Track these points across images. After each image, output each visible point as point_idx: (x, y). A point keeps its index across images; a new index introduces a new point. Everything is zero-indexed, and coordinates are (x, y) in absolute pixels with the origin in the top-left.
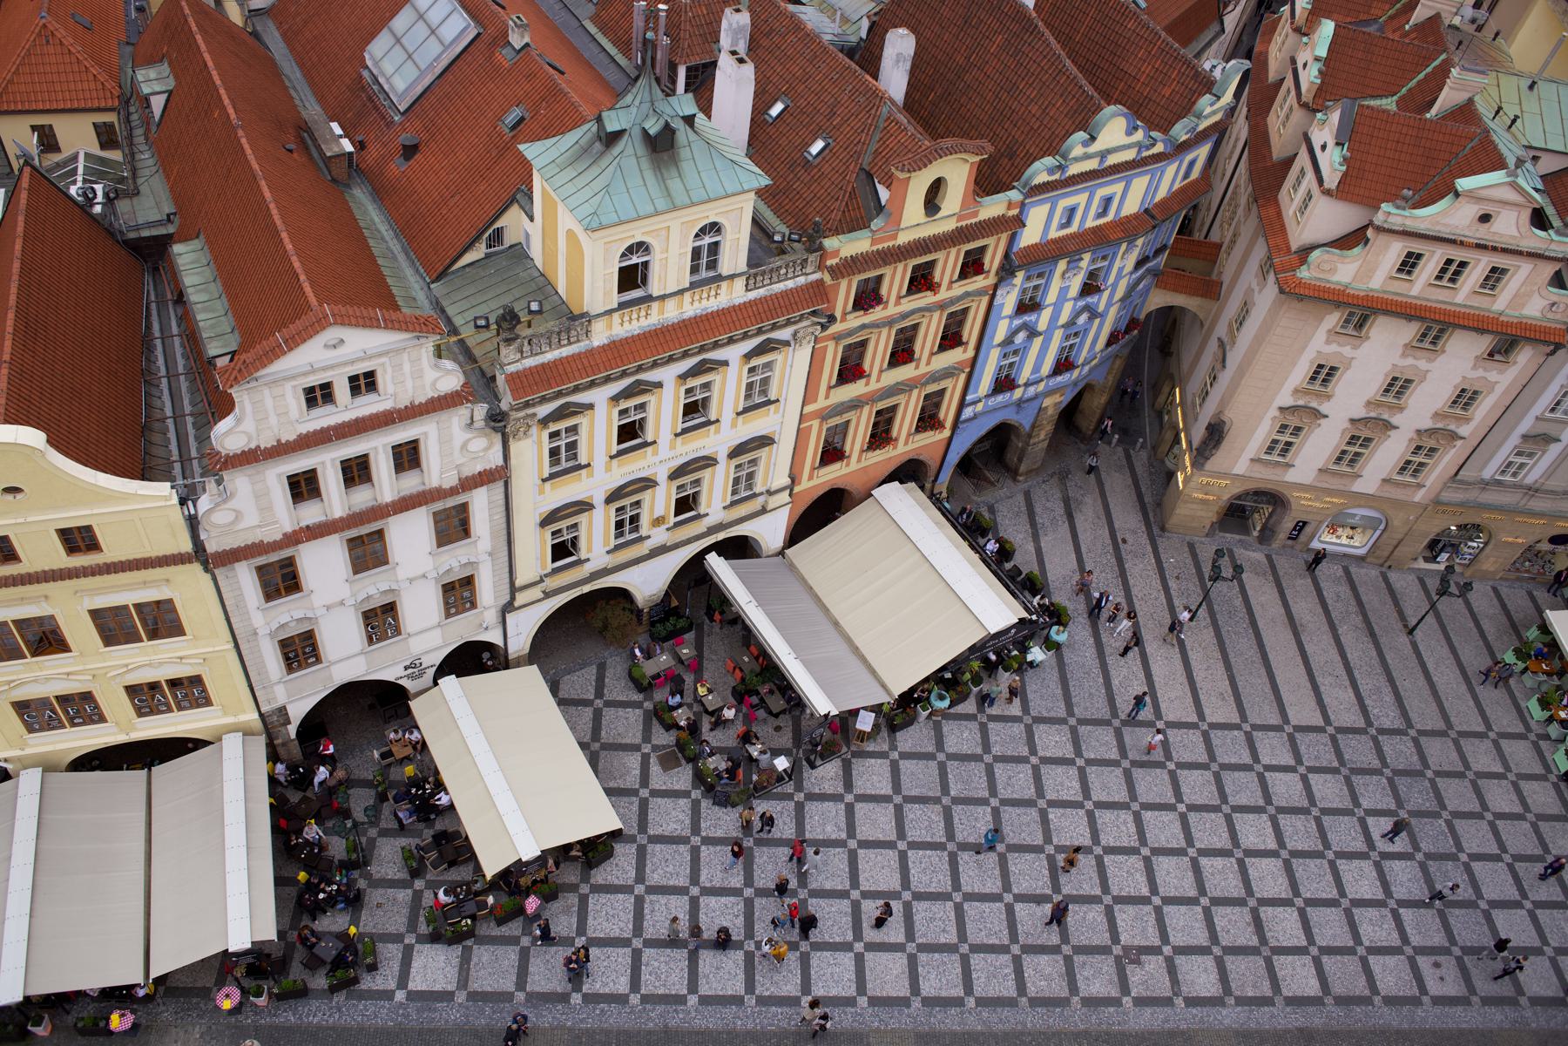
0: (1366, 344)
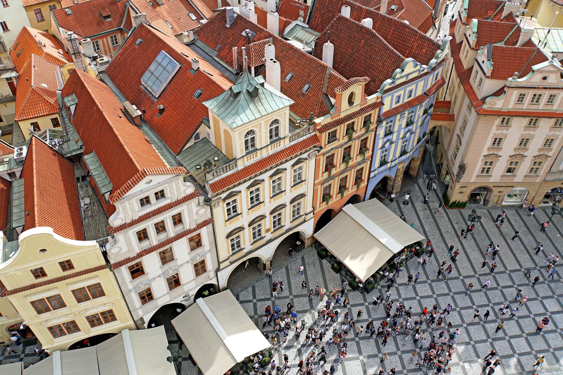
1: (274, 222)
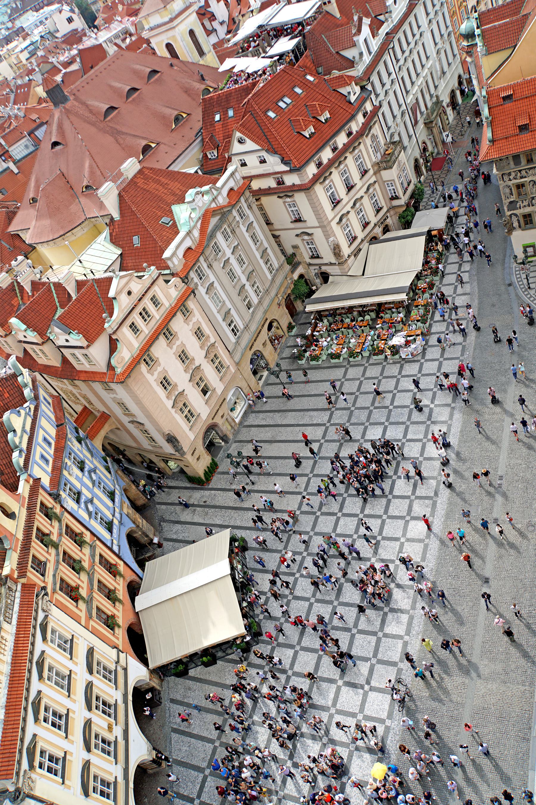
0: (160, 360)
1: (104, 712)
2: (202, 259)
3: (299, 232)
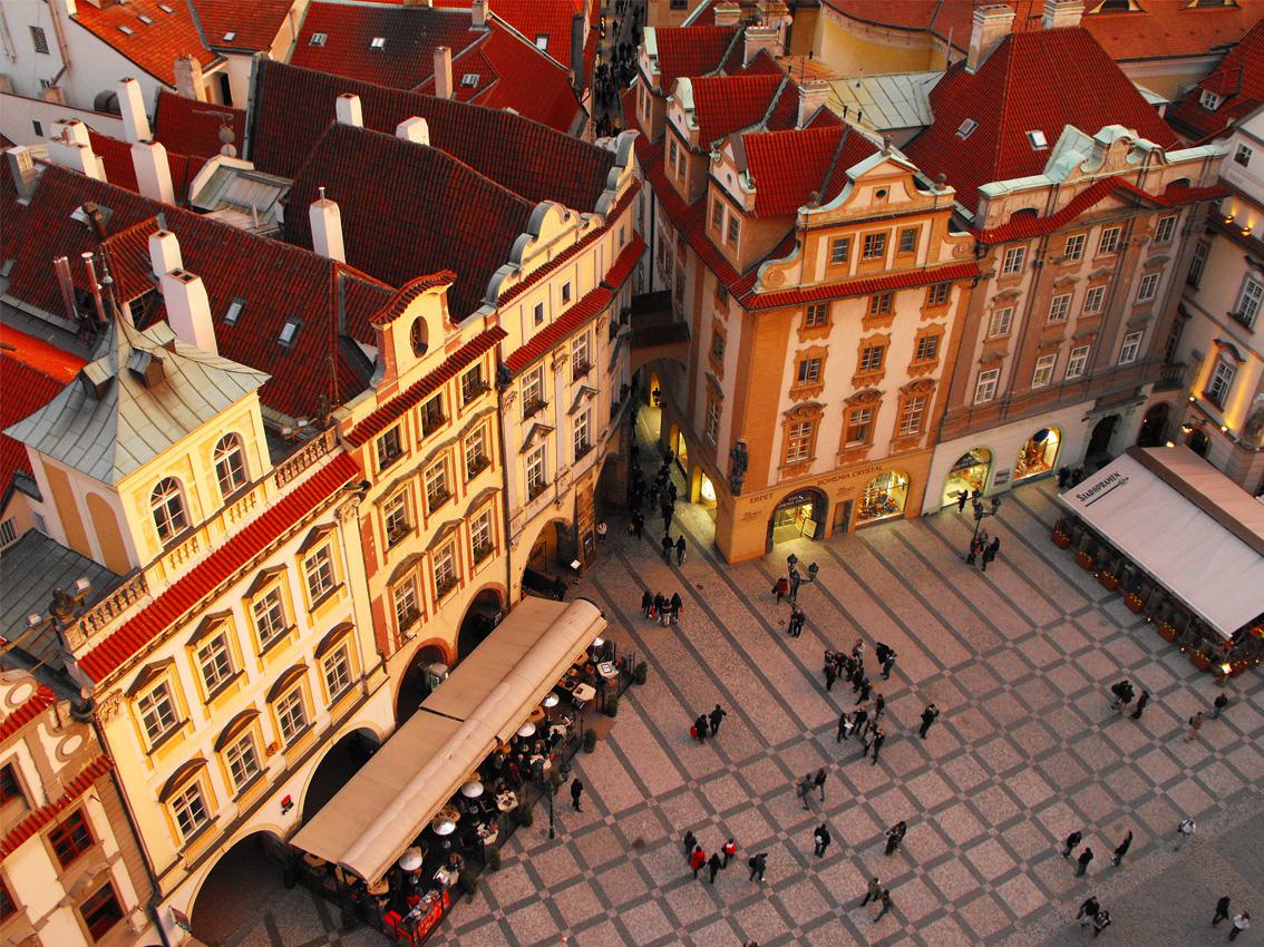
1: (285, 721)
2: (1035, 243)
3: (1226, 338)
